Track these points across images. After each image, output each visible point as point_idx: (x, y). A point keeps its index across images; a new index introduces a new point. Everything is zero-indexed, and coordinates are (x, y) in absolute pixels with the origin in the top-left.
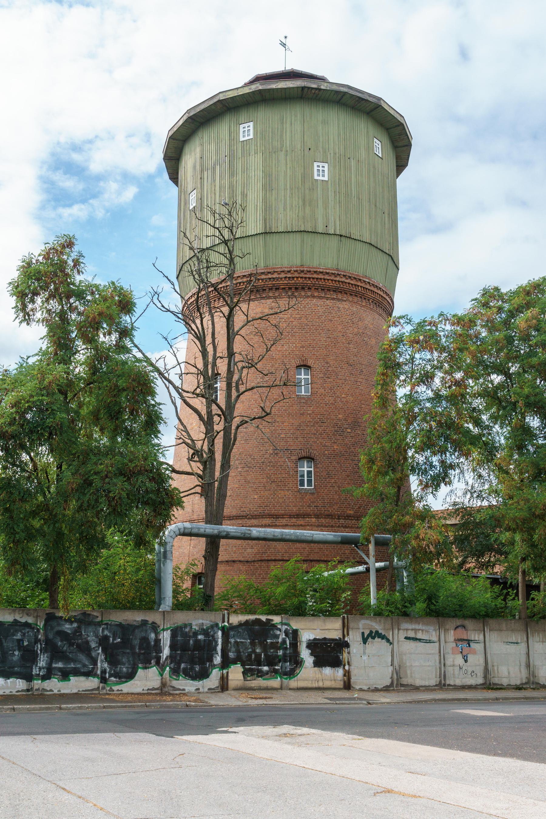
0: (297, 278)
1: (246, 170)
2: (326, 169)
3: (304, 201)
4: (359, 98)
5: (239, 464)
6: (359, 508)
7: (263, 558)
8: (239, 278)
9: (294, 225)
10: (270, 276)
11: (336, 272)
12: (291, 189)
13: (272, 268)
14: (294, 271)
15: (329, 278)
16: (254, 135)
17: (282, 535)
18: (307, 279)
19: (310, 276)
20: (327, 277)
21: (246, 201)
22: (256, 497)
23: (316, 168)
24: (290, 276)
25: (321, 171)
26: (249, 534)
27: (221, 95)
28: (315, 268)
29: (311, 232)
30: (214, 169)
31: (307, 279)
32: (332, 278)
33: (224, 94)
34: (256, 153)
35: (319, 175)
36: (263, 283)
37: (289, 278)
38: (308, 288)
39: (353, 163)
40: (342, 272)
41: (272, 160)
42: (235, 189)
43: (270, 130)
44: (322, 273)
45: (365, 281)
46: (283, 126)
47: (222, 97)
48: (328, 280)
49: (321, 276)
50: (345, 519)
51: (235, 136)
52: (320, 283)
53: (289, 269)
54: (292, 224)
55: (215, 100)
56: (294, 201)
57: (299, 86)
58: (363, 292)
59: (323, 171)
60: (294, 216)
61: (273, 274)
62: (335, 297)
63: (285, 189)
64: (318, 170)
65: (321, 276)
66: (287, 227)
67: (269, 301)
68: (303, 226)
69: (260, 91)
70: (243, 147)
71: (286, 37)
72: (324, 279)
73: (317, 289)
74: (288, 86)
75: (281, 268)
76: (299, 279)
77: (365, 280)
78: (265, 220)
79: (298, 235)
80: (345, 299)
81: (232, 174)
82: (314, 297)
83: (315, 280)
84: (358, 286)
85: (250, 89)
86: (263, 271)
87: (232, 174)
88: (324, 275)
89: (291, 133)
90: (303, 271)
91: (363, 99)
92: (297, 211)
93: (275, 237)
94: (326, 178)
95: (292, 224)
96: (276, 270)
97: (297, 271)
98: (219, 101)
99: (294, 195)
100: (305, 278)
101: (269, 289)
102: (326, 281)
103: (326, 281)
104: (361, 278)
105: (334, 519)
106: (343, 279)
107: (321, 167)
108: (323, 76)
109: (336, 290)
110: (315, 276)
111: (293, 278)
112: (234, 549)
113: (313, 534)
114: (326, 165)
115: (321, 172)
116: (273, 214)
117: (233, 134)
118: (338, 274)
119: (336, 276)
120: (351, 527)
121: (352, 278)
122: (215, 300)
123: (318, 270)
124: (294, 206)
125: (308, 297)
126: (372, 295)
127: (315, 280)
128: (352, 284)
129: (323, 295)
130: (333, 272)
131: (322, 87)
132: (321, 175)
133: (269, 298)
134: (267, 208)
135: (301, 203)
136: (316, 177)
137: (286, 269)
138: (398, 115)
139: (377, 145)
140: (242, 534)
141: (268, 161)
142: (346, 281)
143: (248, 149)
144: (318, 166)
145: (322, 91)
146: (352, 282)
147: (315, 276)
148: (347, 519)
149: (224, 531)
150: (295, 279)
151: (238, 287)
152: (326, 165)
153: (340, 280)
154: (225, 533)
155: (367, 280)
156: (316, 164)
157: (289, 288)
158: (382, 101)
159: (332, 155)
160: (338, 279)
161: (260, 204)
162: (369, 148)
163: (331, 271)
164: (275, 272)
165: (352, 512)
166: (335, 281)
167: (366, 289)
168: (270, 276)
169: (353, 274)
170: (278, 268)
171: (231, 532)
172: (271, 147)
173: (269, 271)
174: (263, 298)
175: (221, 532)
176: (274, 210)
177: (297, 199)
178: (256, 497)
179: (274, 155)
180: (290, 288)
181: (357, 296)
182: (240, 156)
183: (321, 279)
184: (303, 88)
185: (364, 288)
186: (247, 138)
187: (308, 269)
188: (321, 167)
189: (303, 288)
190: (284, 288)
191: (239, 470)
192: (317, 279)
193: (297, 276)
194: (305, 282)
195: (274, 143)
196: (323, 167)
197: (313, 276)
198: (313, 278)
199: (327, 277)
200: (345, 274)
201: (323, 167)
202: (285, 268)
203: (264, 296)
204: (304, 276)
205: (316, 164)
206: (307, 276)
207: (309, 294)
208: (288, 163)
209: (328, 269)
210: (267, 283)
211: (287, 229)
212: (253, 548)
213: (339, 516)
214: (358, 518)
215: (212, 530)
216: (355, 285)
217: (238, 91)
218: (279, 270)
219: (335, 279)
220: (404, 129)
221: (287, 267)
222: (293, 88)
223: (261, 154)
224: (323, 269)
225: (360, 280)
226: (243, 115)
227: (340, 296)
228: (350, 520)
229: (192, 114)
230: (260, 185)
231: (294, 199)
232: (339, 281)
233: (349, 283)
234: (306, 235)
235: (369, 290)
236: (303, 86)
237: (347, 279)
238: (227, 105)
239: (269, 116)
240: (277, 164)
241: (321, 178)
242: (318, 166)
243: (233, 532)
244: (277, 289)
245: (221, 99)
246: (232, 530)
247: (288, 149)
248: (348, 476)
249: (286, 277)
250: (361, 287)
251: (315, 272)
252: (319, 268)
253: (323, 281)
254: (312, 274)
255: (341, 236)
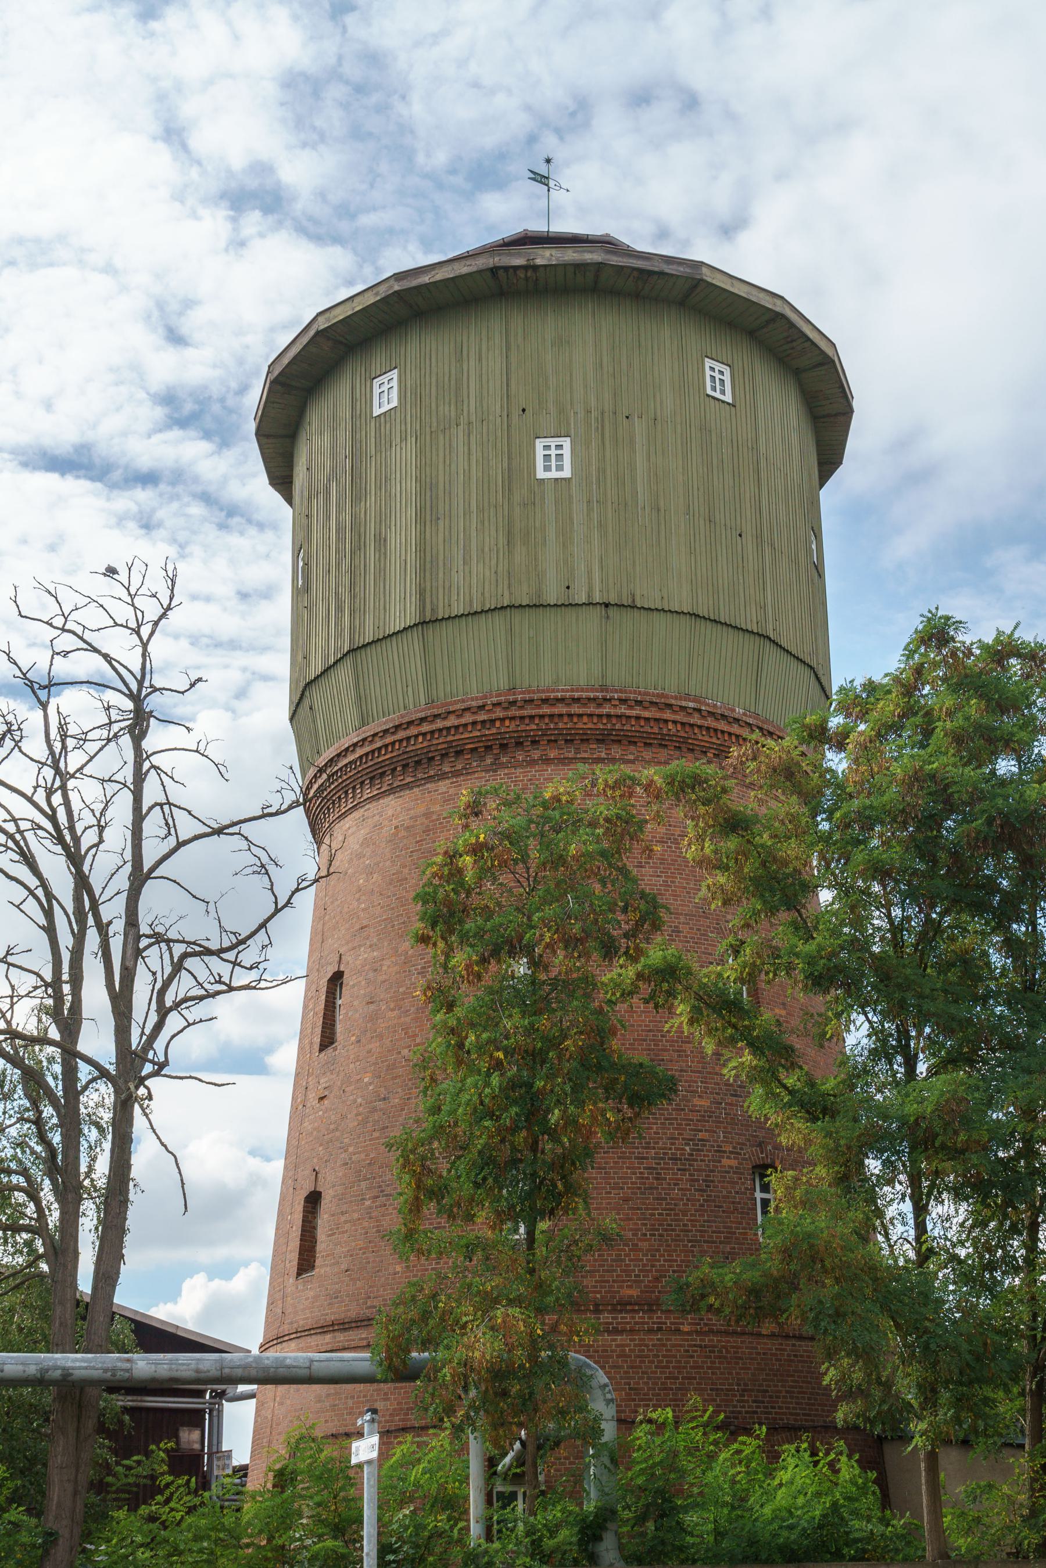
0: (502, 720)
1: (384, 481)
2: (567, 452)
3: (510, 535)
4: (641, 271)
5: (368, 1189)
6: (657, 1279)
7: (409, 1424)
8: (377, 739)
9: (487, 595)
10: (439, 724)
11: (600, 695)
12: (481, 510)
13: (443, 705)
14: (494, 705)
15: (581, 711)
16: (400, 399)
17: (222, 1368)
18: (527, 721)
19: (533, 712)
20: (575, 709)
21: (385, 554)
22: (398, 1268)
23: (540, 453)
24: (485, 717)
25: (553, 458)
26: (127, 1370)
27: (321, 319)
28: (543, 691)
29: (528, 605)
30: (328, 492)
31: (527, 721)
32: (588, 711)
33: (327, 315)
34: (404, 439)
35: (547, 468)
36: (426, 744)
37: (483, 722)
38: (566, 741)
39: (639, 427)
40: (616, 691)
41: (437, 450)
42: (362, 530)
43: (434, 380)
44: (562, 700)
45: (683, 708)
46: (461, 366)
47: (322, 324)
48: (580, 716)
49: (561, 709)
50: (614, 1310)
51: (363, 406)
52: (561, 726)
53: (480, 703)
54: (483, 594)
55: (312, 333)
56: (487, 539)
57: (481, 267)
58: (682, 734)
59: (560, 457)
60: (487, 573)
61: (445, 718)
62: (603, 755)
63: (467, 513)
64: (547, 457)
65: (561, 709)
66: (471, 601)
67: (443, 786)
68: (506, 593)
69: (397, 293)
70: (378, 429)
71: (548, 161)
72: (570, 716)
73: (556, 741)
74: (457, 273)
75: (463, 701)
76: (507, 723)
77: (684, 704)
78: (422, 593)
79: (498, 619)
80: (631, 757)
81: (358, 495)
82: (548, 761)
83: (547, 720)
84: (666, 721)
85: (377, 294)
86: (422, 715)
87: (358, 495)
88: (568, 705)
89: (481, 380)
90: (513, 703)
91: (651, 273)
92: (494, 562)
93: (446, 630)
94: (566, 473)
95: (483, 594)
96: (451, 709)
97: (499, 704)
98: (318, 333)
99: (486, 523)
100: (522, 718)
101: (442, 755)
102: (575, 720)
103: (575, 720)
104: (673, 702)
105: (585, 1312)
106: (623, 710)
107: (553, 447)
108: (608, 235)
109: (603, 739)
110: (546, 710)
111: (493, 721)
112: (350, 1402)
113: (312, 1361)
114: (566, 443)
115: (554, 459)
116: (441, 575)
117: (358, 403)
118: (605, 699)
119: (599, 705)
120: (632, 1331)
121: (647, 704)
122: (339, 797)
123: (552, 695)
124: (487, 549)
125: (532, 763)
126: (714, 740)
127: (547, 720)
128: (647, 719)
129: (570, 755)
130: (592, 695)
131: (539, 262)
132: (554, 468)
133: (443, 776)
134: (427, 563)
135: (502, 541)
136: (541, 474)
137: (474, 704)
138: (762, 295)
139: (717, 376)
140: (106, 1370)
141: (428, 454)
142: (628, 712)
143: (388, 432)
144: (547, 447)
145: (542, 270)
146: (646, 714)
147: (546, 710)
148: (621, 1311)
149: (56, 1368)
150: (498, 724)
151: (376, 761)
152: (566, 443)
153: (613, 711)
154: (58, 1373)
155: (691, 705)
156: (539, 444)
157: (486, 747)
158: (704, 270)
159: (581, 415)
160: (606, 710)
161: (411, 557)
162: (690, 384)
163: (584, 695)
164: (449, 713)
165: (634, 1292)
166: (600, 716)
167: (692, 725)
168: (439, 724)
169: (647, 694)
170: (456, 702)
171: (73, 1368)
172: (434, 419)
173: (436, 711)
174: (430, 779)
175: (47, 1371)
176: (441, 563)
177: (493, 533)
178: (398, 1268)
179: (441, 437)
180: (488, 748)
181: (666, 746)
182: (373, 453)
183: (561, 716)
184: (494, 271)
185: (683, 724)
186: (386, 408)
187: (527, 697)
188: (553, 447)
189: (519, 744)
190: (473, 750)
191: (368, 1203)
192: (551, 716)
193: (501, 715)
194: (522, 727)
195: (441, 408)
196: (559, 447)
197: (541, 712)
198: (542, 717)
199: (575, 709)
200: (623, 696)
201: (559, 447)
202: (472, 699)
203: (432, 773)
204: (518, 713)
205: (539, 444)
206: (525, 713)
207: (536, 754)
208: (473, 446)
209: (577, 691)
210: (435, 742)
211: (484, 605)
212: (388, 1399)
213: (596, 1305)
214: (650, 1305)
215: (21, 1367)
216: (657, 720)
217: (354, 304)
218: (458, 706)
219: (598, 711)
220: (792, 325)
221: (477, 698)
222: (470, 274)
223: (414, 439)
224: (563, 691)
225: (669, 706)
226: (378, 358)
227: (616, 751)
228: (627, 1312)
229: (276, 373)
230: (412, 512)
231: (487, 533)
232: (609, 716)
233: (638, 718)
234: (517, 615)
235: (700, 727)
236: (491, 265)
237: (631, 707)
238: (341, 339)
239: (432, 348)
240: (448, 458)
241: (554, 474)
242: (547, 447)
243: (80, 1368)
244: (459, 753)
245: (322, 327)
246: (78, 1364)
247: (473, 418)
248: (626, 1200)
249: (474, 723)
250: (675, 722)
251: (545, 701)
252: (553, 691)
253: (566, 719)
254: (539, 707)
255: (607, 605)
